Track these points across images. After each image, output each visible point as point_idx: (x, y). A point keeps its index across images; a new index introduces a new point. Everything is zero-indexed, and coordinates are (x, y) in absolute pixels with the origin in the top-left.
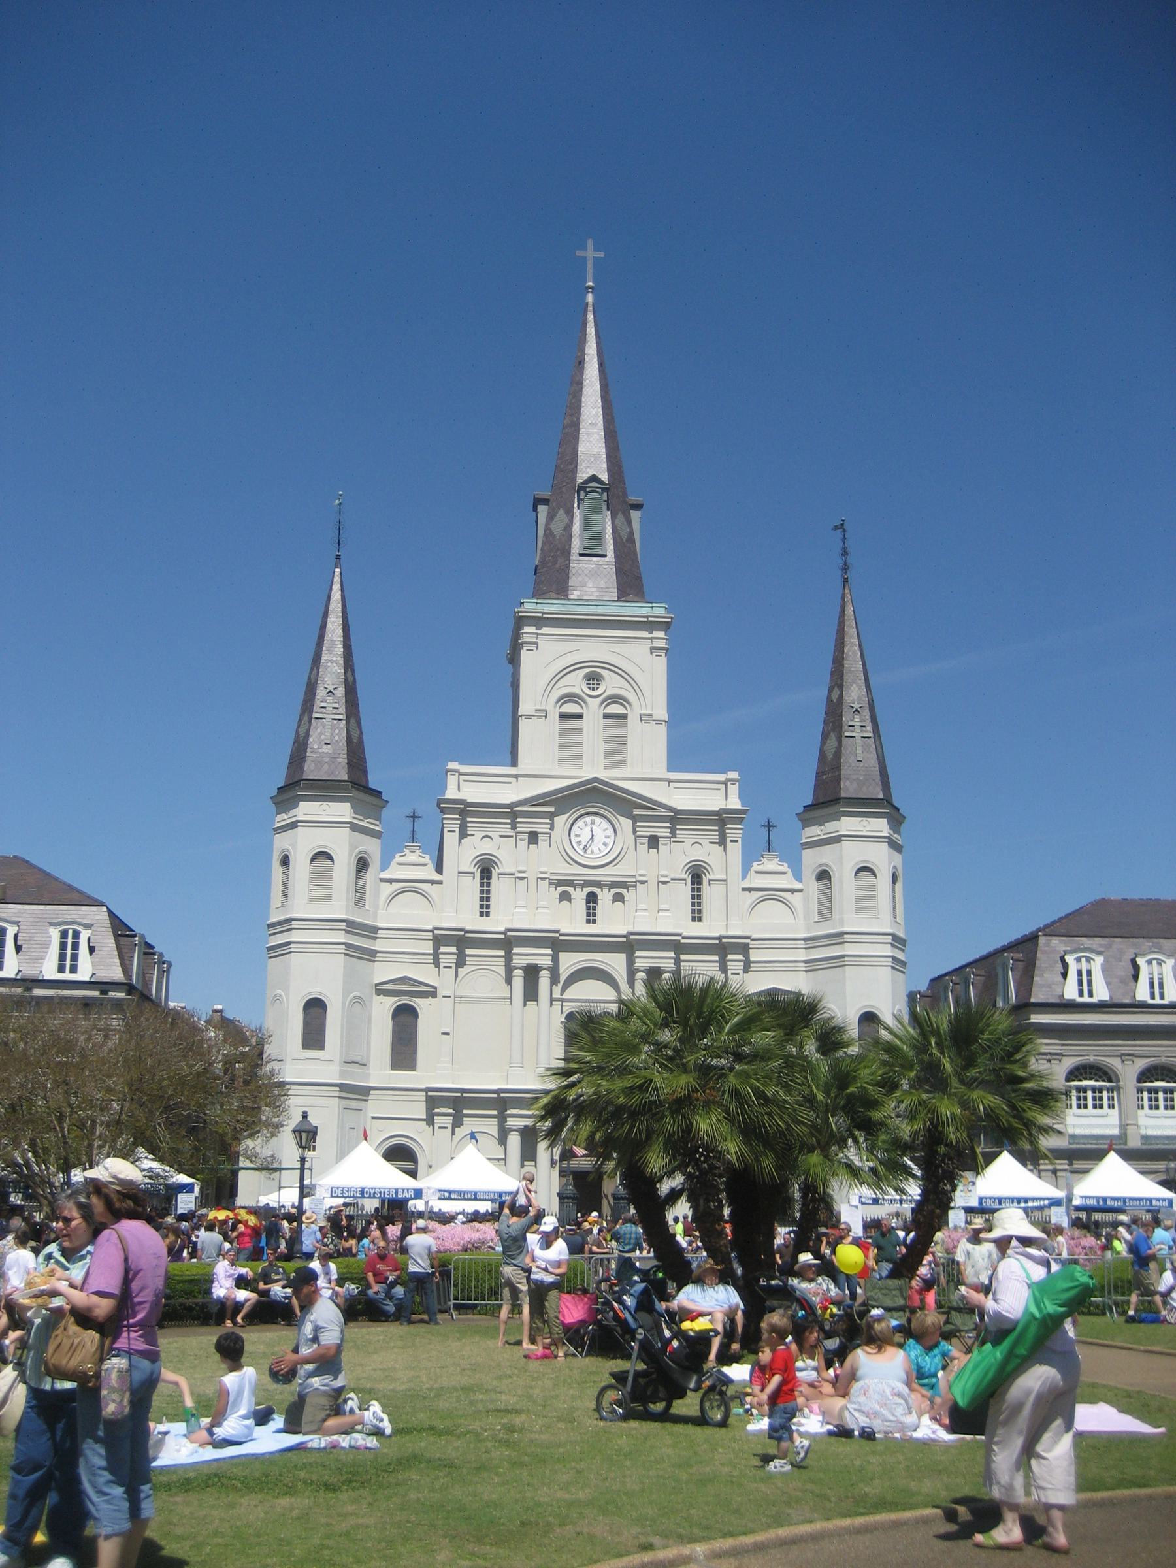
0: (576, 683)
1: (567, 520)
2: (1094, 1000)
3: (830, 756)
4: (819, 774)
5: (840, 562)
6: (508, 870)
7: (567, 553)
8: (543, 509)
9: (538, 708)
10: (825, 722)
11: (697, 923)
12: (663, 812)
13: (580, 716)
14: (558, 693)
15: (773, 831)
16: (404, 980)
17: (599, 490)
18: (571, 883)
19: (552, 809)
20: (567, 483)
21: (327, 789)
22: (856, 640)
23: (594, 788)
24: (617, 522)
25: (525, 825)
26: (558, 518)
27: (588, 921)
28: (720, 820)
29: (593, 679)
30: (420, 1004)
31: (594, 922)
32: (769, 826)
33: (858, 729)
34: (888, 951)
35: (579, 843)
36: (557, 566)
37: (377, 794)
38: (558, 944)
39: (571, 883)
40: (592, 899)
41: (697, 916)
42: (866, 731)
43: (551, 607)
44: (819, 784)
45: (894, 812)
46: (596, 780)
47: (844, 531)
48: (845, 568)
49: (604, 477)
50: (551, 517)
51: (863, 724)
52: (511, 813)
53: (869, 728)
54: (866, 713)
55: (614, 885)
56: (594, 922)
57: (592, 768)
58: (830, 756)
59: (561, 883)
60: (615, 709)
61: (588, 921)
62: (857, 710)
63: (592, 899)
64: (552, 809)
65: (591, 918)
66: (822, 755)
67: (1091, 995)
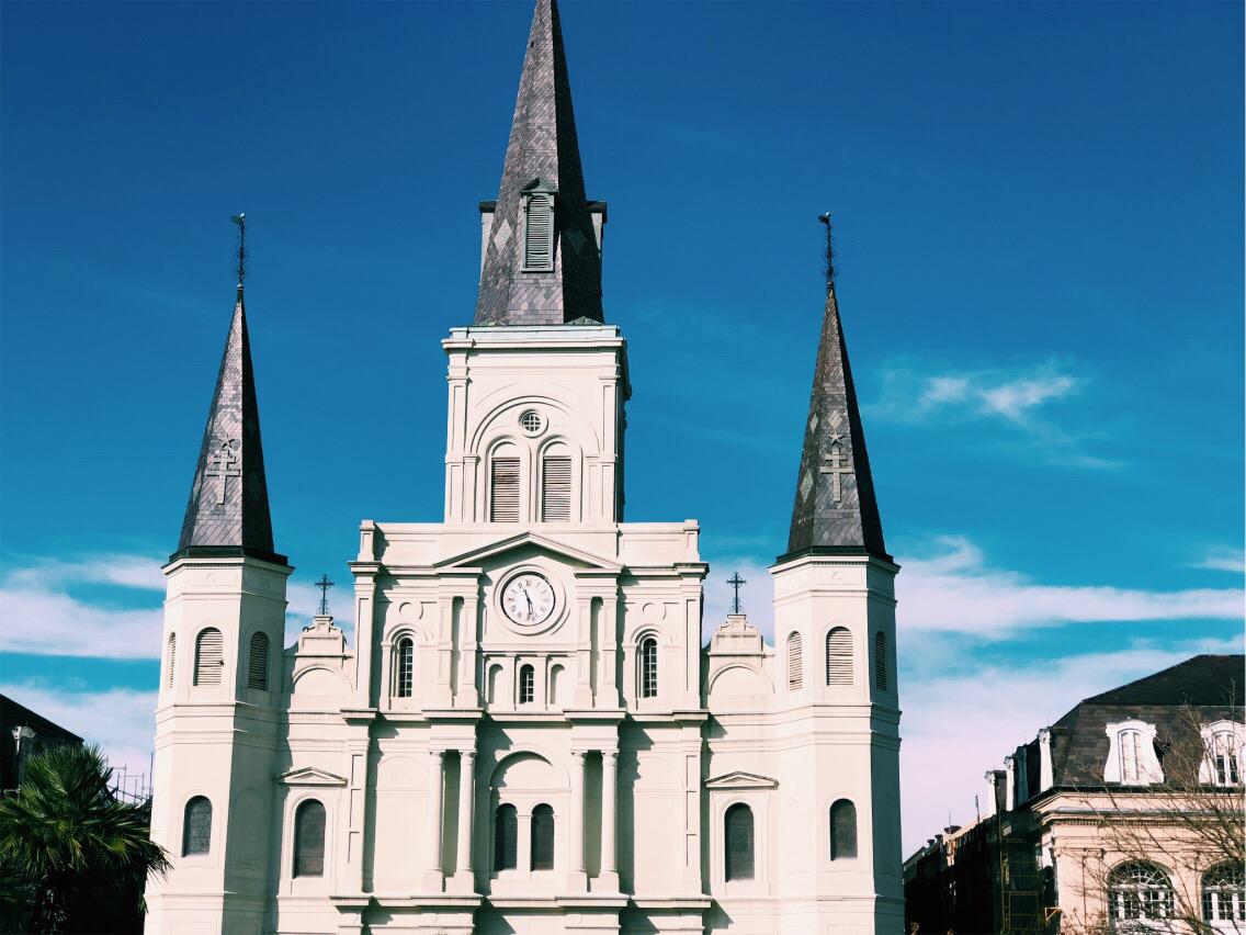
0: (509, 423)
1: (510, 232)
3: (805, 497)
4: (795, 518)
5: (823, 265)
6: (430, 642)
7: (509, 272)
8: (488, 218)
9: (467, 453)
10: (804, 457)
11: (651, 698)
13: (517, 461)
15: (742, 588)
17: (545, 195)
18: (501, 655)
19: (479, 570)
20: (513, 189)
22: (839, 358)
23: (531, 549)
26: (501, 231)
27: (523, 700)
28: (678, 572)
31: (531, 699)
32: (736, 582)
33: (836, 465)
34: (811, 725)
35: (514, 608)
36: (498, 286)
37: (282, 560)
39: (501, 655)
41: (649, 689)
42: (846, 466)
43: (485, 336)
44: (795, 530)
45: (879, 562)
46: (527, 534)
47: (829, 228)
48: (830, 272)
49: (553, 179)
50: (495, 229)
51: (844, 457)
53: (851, 461)
54: (847, 441)
56: (531, 699)
57: (525, 523)
58: (805, 497)
61: (523, 700)
62: (836, 442)
63: (527, 670)
64: (479, 570)
65: (525, 695)
66: (799, 495)
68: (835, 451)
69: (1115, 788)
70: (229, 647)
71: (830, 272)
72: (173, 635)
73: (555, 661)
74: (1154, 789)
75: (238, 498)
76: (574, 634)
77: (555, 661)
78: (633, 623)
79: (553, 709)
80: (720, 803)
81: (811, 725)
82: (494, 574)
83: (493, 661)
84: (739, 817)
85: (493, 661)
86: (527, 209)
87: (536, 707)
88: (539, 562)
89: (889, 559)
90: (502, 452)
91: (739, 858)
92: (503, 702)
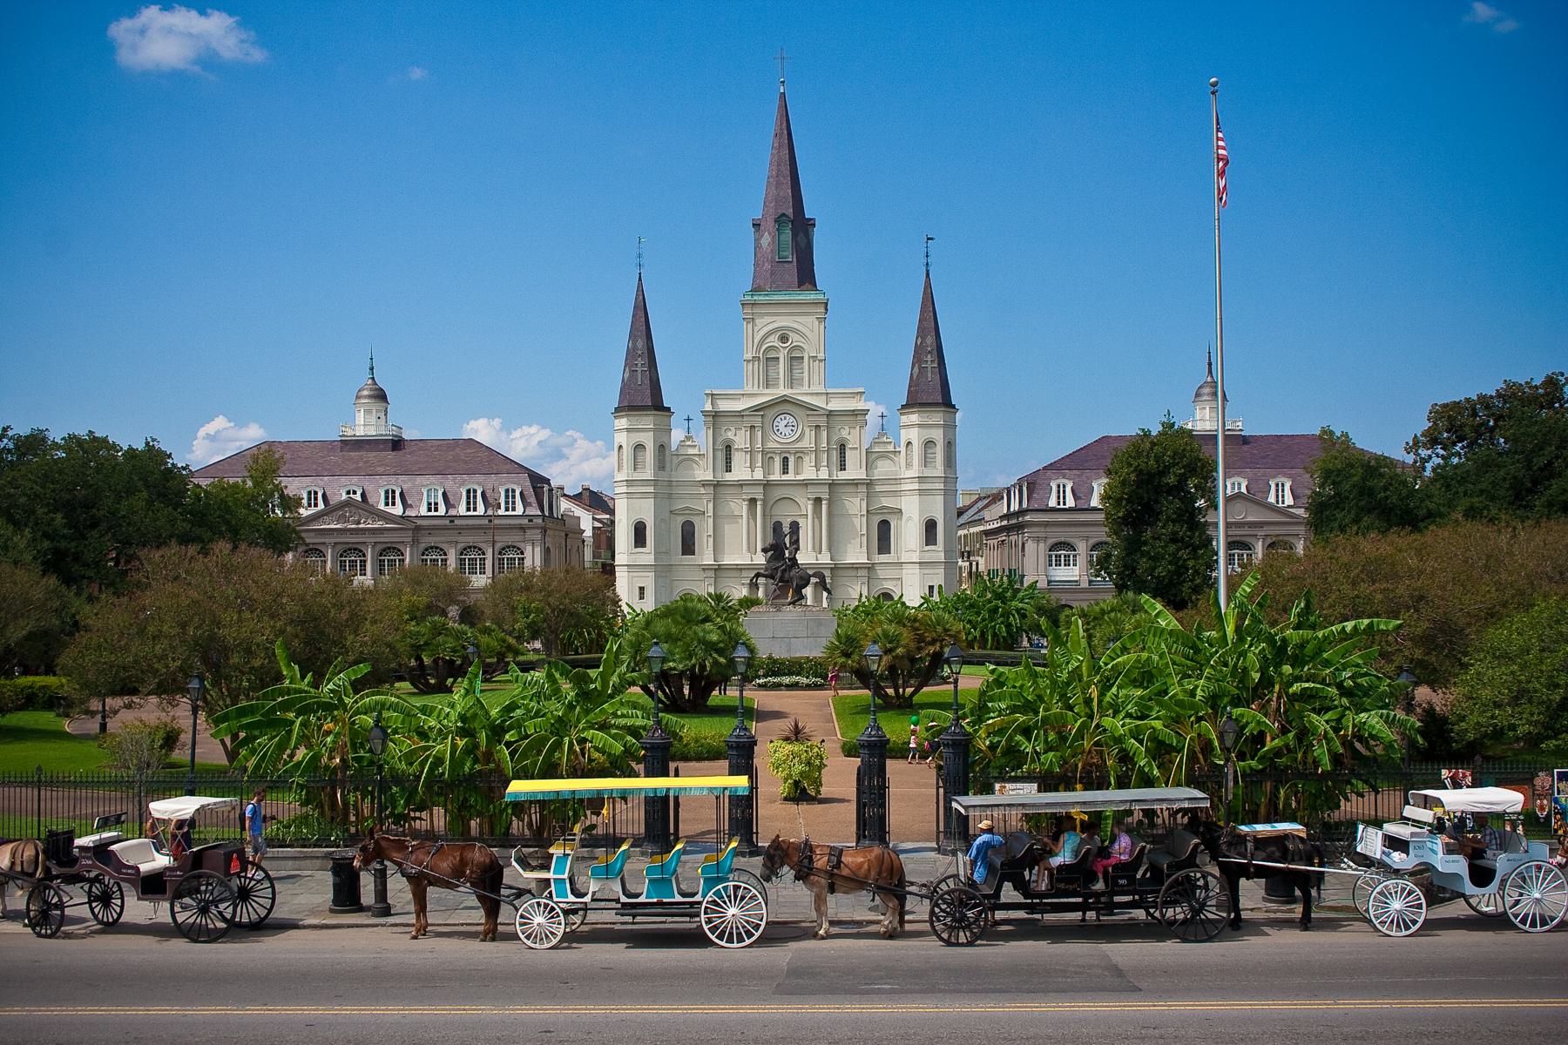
0: (774, 341)
2: (1067, 507)
4: (910, 386)
12: (823, 412)
14: (764, 348)
16: (688, 508)
21: (643, 410)
23: (784, 401)
24: (799, 238)
25: (748, 422)
29: (784, 339)
30: (696, 520)
37: (668, 409)
38: (767, 485)
40: (786, 460)
41: (843, 467)
48: (927, 264)
52: (739, 415)
54: (935, 352)
55: (797, 452)
57: (781, 391)
59: (768, 452)
60: (797, 354)
63: (786, 460)
65: (785, 471)
67: (1064, 504)
68: (929, 356)
69: (1053, 510)
70: (649, 455)
71: (927, 264)
72: (621, 446)
73: (798, 455)
74: (1070, 510)
75: (647, 382)
76: (808, 442)
77: (798, 455)
78: (835, 438)
79: (799, 477)
80: (877, 519)
81: (916, 486)
82: (771, 413)
83: (769, 455)
84: (884, 527)
85: (769, 455)
86: (778, 230)
87: (790, 476)
88: (788, 408)
89: (954, 407)
90: (772, 355)
91: (884, 543)
92: (776, 476)
